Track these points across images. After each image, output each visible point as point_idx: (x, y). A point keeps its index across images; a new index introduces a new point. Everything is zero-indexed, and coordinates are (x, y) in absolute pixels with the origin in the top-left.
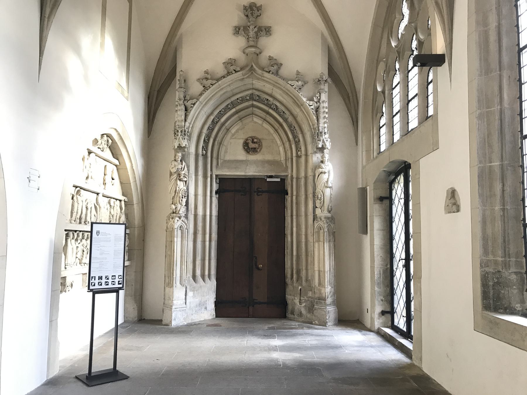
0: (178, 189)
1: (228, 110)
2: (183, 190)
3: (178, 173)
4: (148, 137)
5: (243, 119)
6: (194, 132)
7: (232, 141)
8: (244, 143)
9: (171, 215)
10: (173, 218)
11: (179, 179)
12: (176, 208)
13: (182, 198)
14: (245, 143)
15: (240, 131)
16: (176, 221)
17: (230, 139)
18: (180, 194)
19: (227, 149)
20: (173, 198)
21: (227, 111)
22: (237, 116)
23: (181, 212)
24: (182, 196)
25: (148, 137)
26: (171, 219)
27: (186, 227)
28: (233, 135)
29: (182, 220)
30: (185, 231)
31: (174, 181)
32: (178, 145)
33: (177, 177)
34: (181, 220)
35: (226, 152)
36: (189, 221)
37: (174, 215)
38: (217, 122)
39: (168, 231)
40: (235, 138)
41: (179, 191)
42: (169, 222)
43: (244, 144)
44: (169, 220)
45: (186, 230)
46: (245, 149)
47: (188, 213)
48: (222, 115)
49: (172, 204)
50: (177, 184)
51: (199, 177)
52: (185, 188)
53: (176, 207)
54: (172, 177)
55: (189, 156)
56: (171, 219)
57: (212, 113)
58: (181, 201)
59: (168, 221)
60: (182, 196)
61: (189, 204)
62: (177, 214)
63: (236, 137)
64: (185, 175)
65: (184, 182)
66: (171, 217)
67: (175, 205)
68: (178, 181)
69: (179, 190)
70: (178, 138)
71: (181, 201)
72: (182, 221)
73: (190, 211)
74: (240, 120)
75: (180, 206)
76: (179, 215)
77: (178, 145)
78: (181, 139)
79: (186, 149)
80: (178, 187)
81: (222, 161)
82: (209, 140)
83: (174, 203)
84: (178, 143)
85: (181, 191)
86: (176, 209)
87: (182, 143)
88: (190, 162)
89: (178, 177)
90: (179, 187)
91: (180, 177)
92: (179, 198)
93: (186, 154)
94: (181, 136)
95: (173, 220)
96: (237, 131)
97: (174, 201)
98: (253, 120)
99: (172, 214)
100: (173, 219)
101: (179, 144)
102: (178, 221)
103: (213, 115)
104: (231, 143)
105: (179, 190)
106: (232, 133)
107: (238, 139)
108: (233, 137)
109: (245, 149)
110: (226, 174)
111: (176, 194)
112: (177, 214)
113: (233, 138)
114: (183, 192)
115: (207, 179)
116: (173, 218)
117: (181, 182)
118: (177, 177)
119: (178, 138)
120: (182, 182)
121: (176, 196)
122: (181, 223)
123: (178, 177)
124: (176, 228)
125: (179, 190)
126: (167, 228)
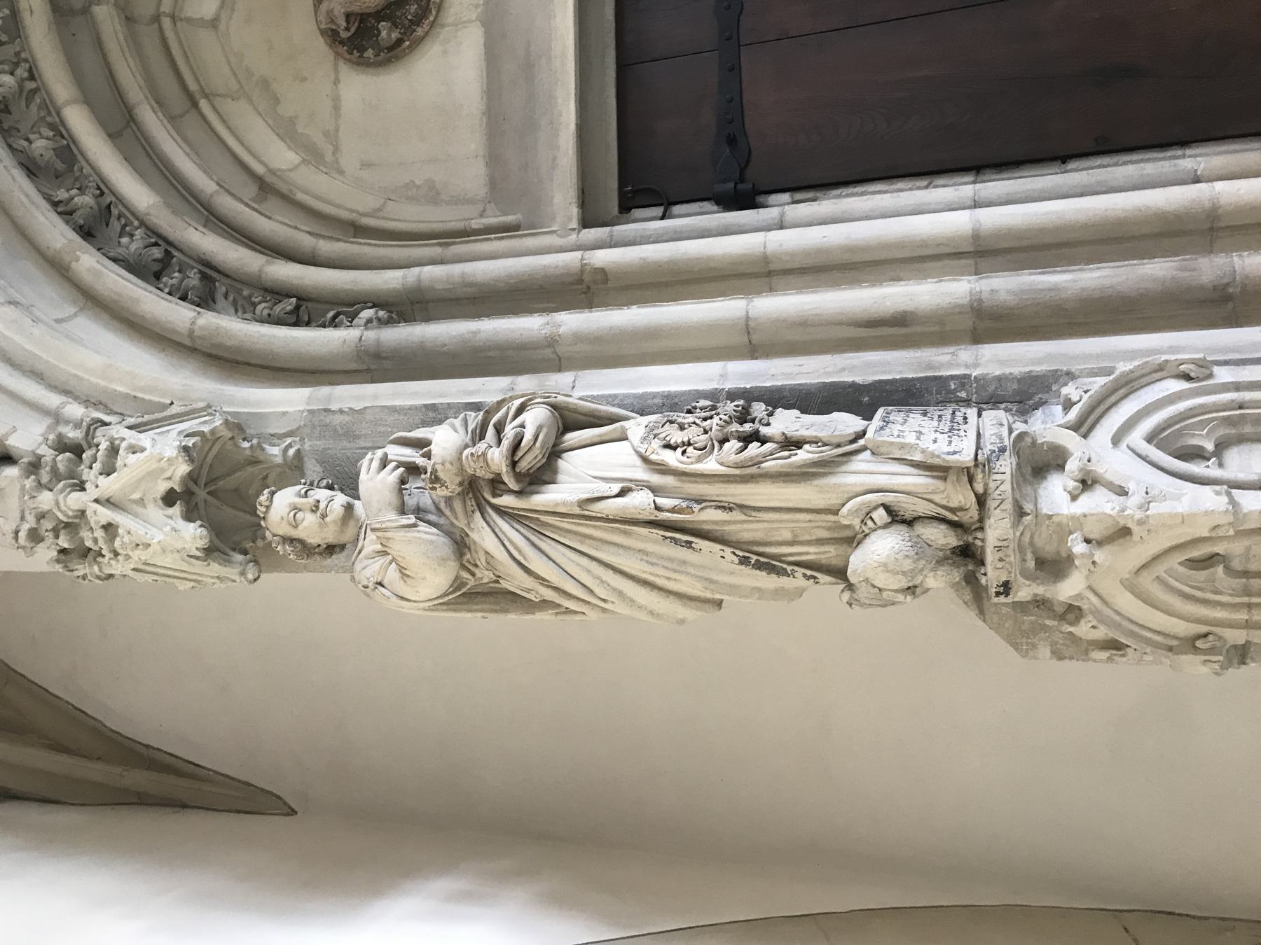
0: (640, 501)
1: (84, 163)
2: (656, 444)
3: (458, 505)
4: (293, 812)
5: (193, 86)
6: (142, 389)
7: (349, 161)
8: (362, 63)
9: (1006, 588)
10: (1041, 563)
11: (519, 494)
12: (896, 518)
13: (755, 437)
14: (362, 50)
15: (286, 110)
16: (1098, 503)
17: (341, 172)
18: (711, 465)
19: (410, 193)
20: (771, 565)
21: (87, 170)
22: (150, 119)
23: (963, 449)
24: (734, 445)
25: (293, 812)
26: (1068, 589)
27: (1175, 386)
28: (313, 155)
29: (1076, 427)
30: (1237, 387)
31: (545, 545)
32: (177, 510)
33: (500, 511)
34: (1070, 440)
35: (432, 195)
36: (1075, 368)
37: (998, 529)
38: (158, 238)
39: (1237, 637)
40: (333, 136)
41: (669, 480)
42: (1103, 620)
43: (369, 53)
44: (1073, 612)
45: (1223, 375)
46: (399, 42)
47: (963, 380)
48: (115, 211)
49: (840, 573)
50: (585, 510)
51: (561, 330)
52: (636, 427)
53: (880, 515)
54: (516, 581)
55: (339, 419)
56: (1068, 589)
57: (59, 268)
58: (804, 455)
59: (1083, 629)
60: (734, 445)
61: (848, 378)
62: (981, 500)
63: (326, 134)
64: (491, 431)
65: (572, 437)
66: (1024, 591)
67: (853, 540)
68: (549, 497)
69: (655, 490)
70: (107, 514)
71: (804, 455)
72: (1084, 426)
73: (930, 367)
74: (195, 105)
75: (862, 462)
76: (1006, 465)
77: (177, 510)
78: (108, 486)
79: (275, 451)
80: (622, 493)
81: (491, 208)
82: (277, 293)
83: (829, 554)
84: (157, 513)
85: (672, 459)
86: (910, 523)
87: (152, 475)
88: (397, 403)
89: (506, 501)
90: (616, 488)
91: (496, 484)
92: (749, 474)
93: (320, 444)
94: (81, 487)
95: (1079, 548)
96: (287, 132)
97: (812, 553)
98: (214, 23)
99: (992, 575)
100: (1070, 558)
101: (169, 499)
102: (1087, 483)
103: (67, 258)
104: (366, 165)
105: (656, 479)
106: (296, 168)
107: (337, 108)
108: (328, 149)
109: (399, 42)
110: (573, 127)
111: (709, 516)
112: (981, 500)
113: (336, 150)
114: (677, 437)
115: (602, 275)
116: (1041, 563)
117: (562, 464)
118: (500, 511)
119: (107, 514)
120: (570, 463)
121: (748, 530)
122: (1116, 441)
123: (506, 501)
124: (1232, 501)
125: (656, 479)
126: (1190, 644)
